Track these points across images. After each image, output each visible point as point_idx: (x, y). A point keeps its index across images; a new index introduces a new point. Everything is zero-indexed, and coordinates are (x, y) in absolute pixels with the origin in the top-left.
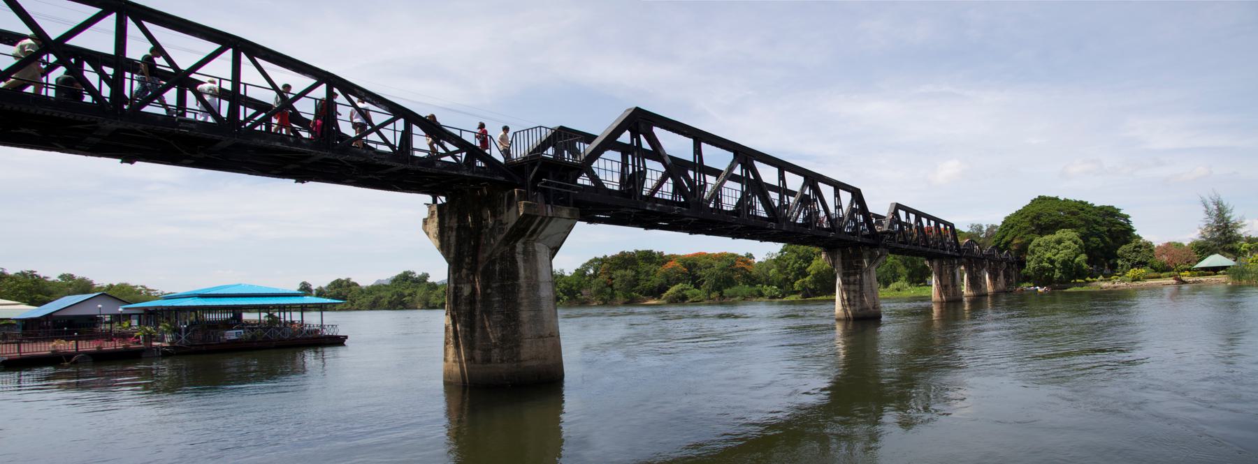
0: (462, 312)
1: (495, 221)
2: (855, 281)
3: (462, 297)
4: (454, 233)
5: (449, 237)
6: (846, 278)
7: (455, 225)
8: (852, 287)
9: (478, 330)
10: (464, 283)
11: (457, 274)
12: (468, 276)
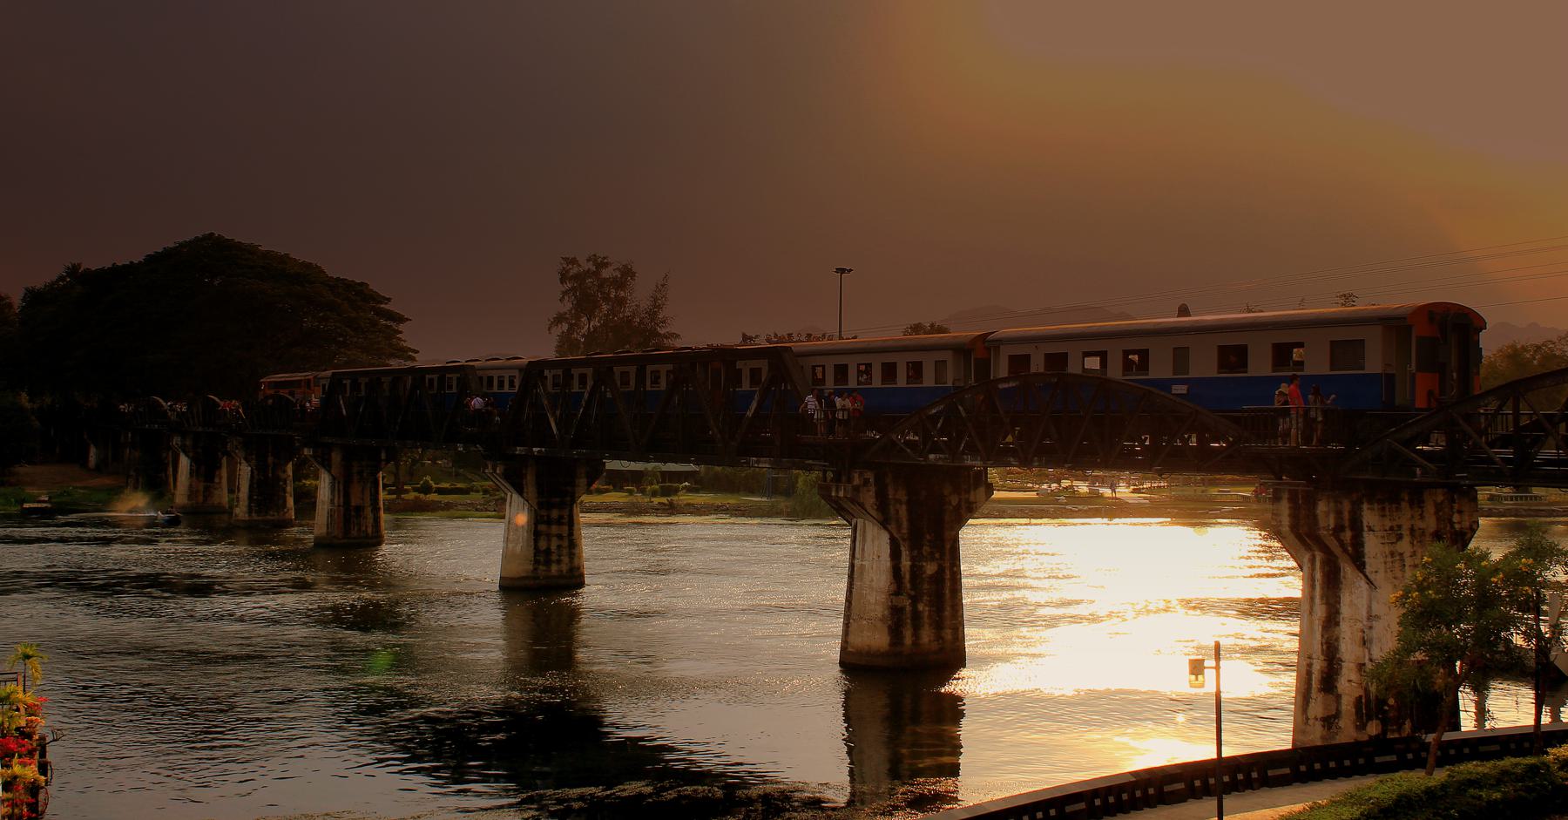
0: (925, 591)
1: (960, 500)
2: (561, 517)
3: (924, 576)
4: (904, 507)
5: (897, 511)
6: (544, 513)
7: (904, 498)
8: (554, 529)
9: (948, 609)
10: (926, 561)
11: (915, 553)
12: (932, 553)
